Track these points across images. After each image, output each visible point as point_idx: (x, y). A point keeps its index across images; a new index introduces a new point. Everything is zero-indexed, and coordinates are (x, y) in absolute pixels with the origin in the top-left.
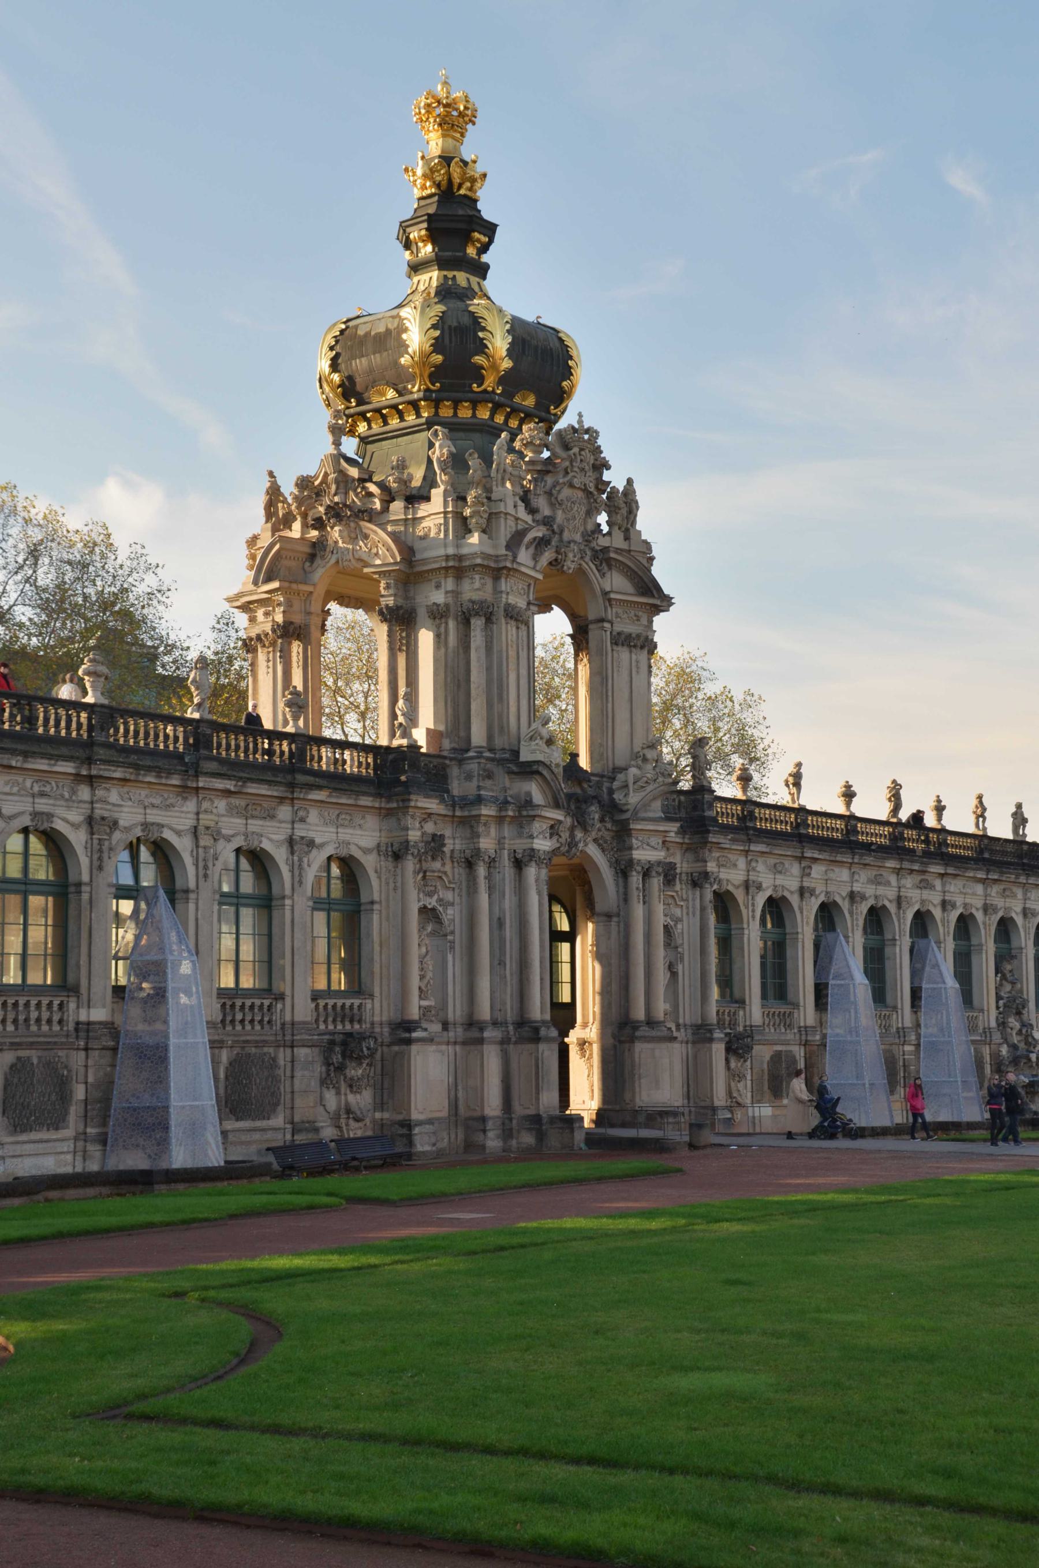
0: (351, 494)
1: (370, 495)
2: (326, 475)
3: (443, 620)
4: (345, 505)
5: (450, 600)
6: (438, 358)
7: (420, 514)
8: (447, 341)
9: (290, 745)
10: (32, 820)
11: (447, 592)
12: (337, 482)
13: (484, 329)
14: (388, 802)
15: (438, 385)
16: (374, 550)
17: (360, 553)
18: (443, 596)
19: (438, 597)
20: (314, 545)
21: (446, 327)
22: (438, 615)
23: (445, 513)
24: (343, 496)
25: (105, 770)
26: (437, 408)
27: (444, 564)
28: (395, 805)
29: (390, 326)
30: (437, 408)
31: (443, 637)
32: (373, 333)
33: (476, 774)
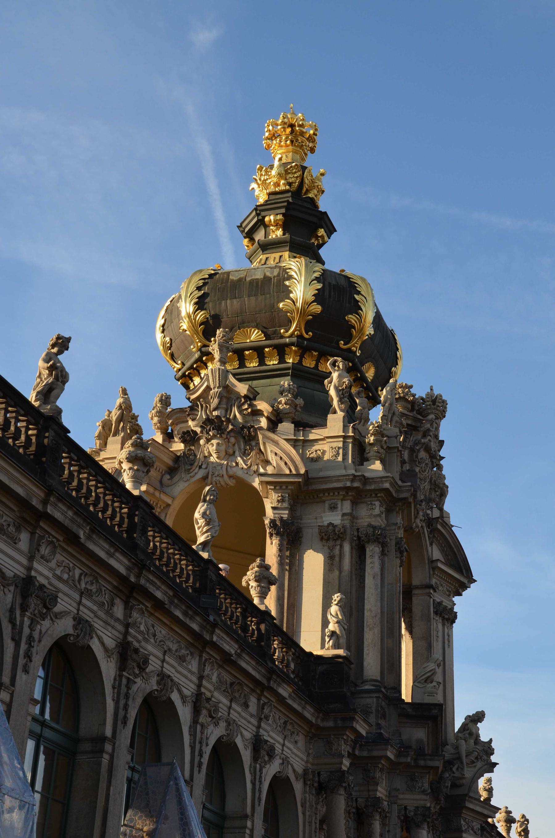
0: (235, 410)
1: (257, 413)
2: (208, 388)
3: (338, 542)
4: (228, 421)
5: (347, 523)
6: (317, 308)
7: (312, 437)
8: (327, 293)
9: (258, 624)
10: (75, 627)
11: (344, 515)
12: (221, 397)
13: (359, 293)
14: (323, 720)
15: (310, 333)
16: (254, 468)
17: (234, 469)
18: (340, 517)
19: (335, 518)
20: (177, 459)
21: (326, 283)
22: (329, 538)
23: (345, 437)
24: (223, 412)
25: (153, 583)
26: (302, 357)
27: (348, 484)
28: (331, 724)
29: (268, 274)
30: (302, 357)
31: (337, 559)
32: (248, 279)
33: (374, 709)
